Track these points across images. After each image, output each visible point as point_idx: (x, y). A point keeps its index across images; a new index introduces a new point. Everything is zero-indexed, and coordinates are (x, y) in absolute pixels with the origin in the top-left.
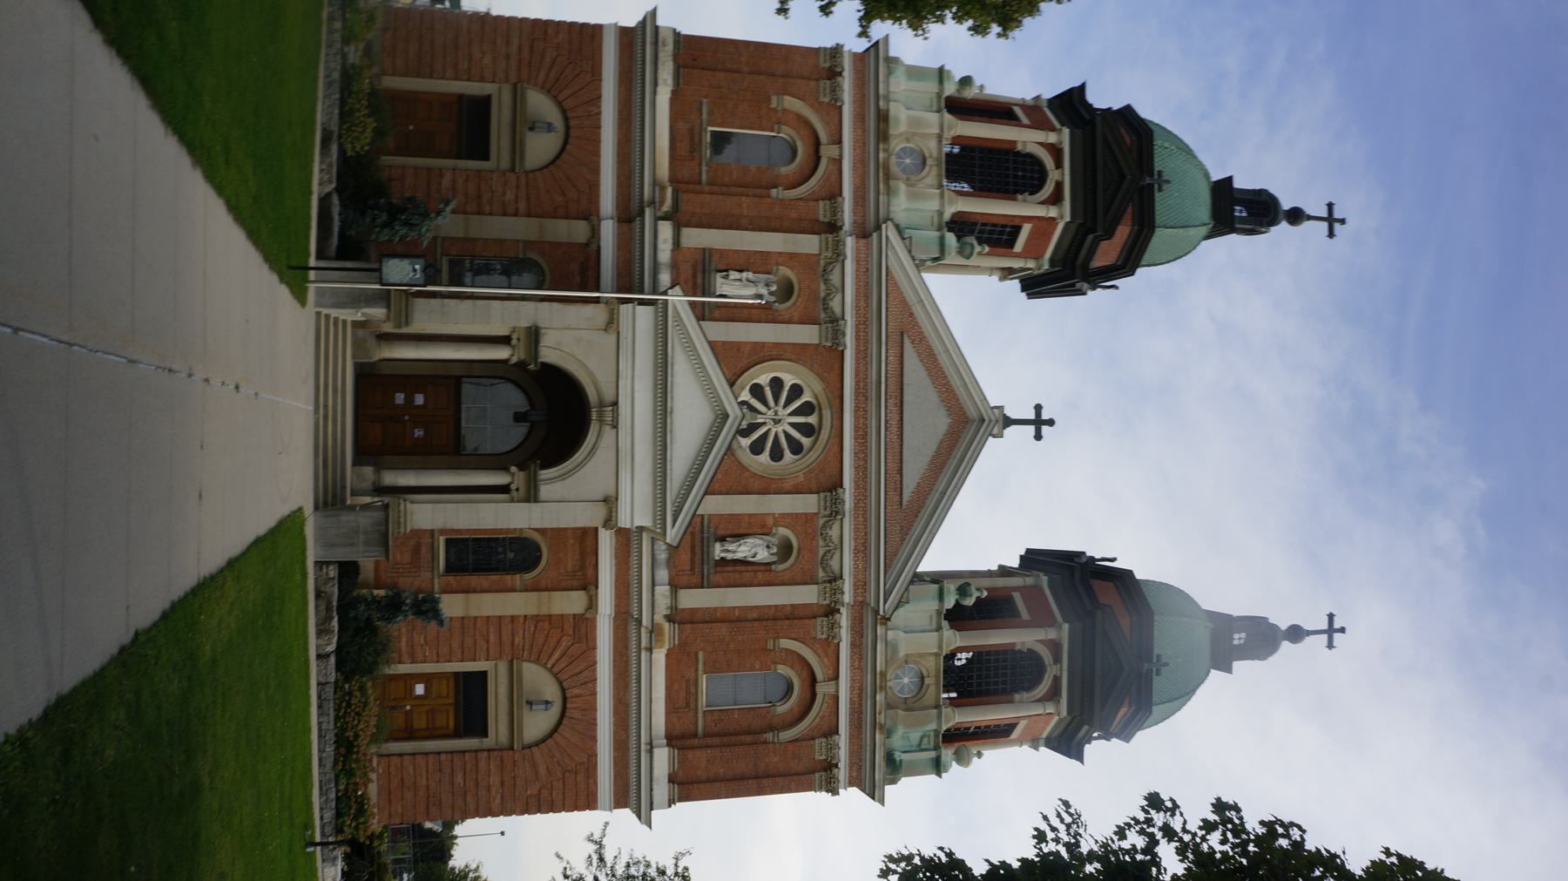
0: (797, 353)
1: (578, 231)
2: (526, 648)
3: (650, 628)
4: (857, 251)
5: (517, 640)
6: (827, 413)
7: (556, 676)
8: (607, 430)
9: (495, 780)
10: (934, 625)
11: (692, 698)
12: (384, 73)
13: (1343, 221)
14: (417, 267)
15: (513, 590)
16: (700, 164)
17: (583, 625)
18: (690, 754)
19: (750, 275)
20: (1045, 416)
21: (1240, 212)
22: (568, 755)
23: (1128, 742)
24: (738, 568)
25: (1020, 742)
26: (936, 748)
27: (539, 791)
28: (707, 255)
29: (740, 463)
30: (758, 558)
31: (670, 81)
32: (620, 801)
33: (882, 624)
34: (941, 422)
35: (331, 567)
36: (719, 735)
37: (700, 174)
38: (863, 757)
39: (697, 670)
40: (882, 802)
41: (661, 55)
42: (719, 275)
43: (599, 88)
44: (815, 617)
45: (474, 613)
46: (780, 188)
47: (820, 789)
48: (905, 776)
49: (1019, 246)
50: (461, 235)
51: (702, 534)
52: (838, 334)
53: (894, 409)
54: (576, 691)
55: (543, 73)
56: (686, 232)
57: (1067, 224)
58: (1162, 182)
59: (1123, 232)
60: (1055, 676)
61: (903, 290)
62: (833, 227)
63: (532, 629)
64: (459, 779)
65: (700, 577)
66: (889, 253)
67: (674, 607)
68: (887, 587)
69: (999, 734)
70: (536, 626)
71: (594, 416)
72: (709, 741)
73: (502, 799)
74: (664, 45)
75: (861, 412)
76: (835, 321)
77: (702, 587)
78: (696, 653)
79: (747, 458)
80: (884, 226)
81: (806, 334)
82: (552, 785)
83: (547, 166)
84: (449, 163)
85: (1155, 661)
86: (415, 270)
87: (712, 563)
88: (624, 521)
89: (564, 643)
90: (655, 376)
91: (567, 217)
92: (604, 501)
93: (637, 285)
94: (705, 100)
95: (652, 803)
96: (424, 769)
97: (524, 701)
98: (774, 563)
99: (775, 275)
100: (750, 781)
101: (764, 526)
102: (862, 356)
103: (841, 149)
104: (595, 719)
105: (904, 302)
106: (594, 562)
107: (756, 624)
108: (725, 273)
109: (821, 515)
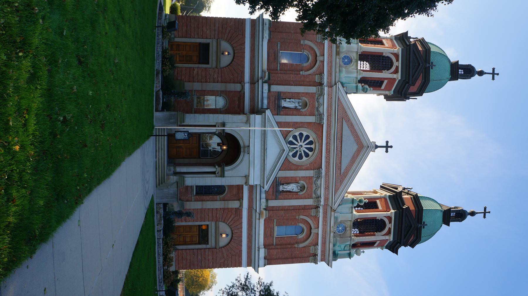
0: (308, 125)
1: (238, 87)
2: (220, 218)
3: (259, 213)
4: (328, 92)
5: (218, 215)
6: (317, 145)
7: (230, 226)
8: (246, 154)
9: (210, 257)
10: (350, 212)
11: (272, 233)
12: (175, 37)
13: (498, 74)
14: (186, 134)
15: (217, 200)
16: (277, 64)
17: (238, 211)
18: (271, 251)
19: (293, 100)
20: (389, 145)
21: (461, 72)
22: (233, 250)
23: (413, 248)
24: (287, 194)
25: (378, 246)
26: (349, 250)
27: (224, 261)
28: (279, 94)
29: (289, 161)
30: (294, 190)
31: (267, 37)
32: (249, 264)
33: (333, 212)
34: (355, 147)
35: (161, 205)
36: (280, 245)
37: (277, 67)
38: (326, 252)
39: (274, 225)
40: (331, 267)
41: (264, 28)
42: (283, 100)
43: (244, 40)
44: (312, 209)
45: (204, 207)
46: (303, 71)
47: (312, 262)
48: (339, 258)
49: (383, 87)
50: (200, 89)
51: (277, 182)
52: (321, 119)
53: (339, 143)
54: (236, 231)
55: (226, 35)
56: (272, 87)
57: (399, 80)
58: (433, 65)
59: (419, 83)
60: (389, 228)
61: (343, 104)
62: (321, 84)
63: (222, 212)
64: (200, 257)
65: (275, 196)
66: (339, 92)
67: (267, 206)
68: (335, 200)
69: (370, 245)
70: (224, 211)
71: (242, 150)
72: (277, 247)
73: (213, 263)
74: (266, 25)
75: (328, 144)
76: (321, 116)
77: (276, 199)
78: (274, 220)
79: (292, 159)
80: (337, 84)
81: (311, 119)
82: (228, 260)
83: (227, 66)
84: (197, 65)
85: (423, 223)
86: (185, 135)
87: (279, 192)
88: (251, 183)
89: (232, 217)
90: (262, 138)
91: (234, 83)
92: (245, 177)
93: (256, 107)
94: (279, 42)
95: (259, 266)
96: (189, 254)
97: (220, 234)
98: (299, 192)
99: (301, 99)
100: (290, 259)
101: (296, 180)
102: (329, 126)
103: (324, 57)
104: (242, 240)
105: (344, 108)
106: (242, 192)
107: (293, 211)
108: (285, 100)
109: (315, 177)
